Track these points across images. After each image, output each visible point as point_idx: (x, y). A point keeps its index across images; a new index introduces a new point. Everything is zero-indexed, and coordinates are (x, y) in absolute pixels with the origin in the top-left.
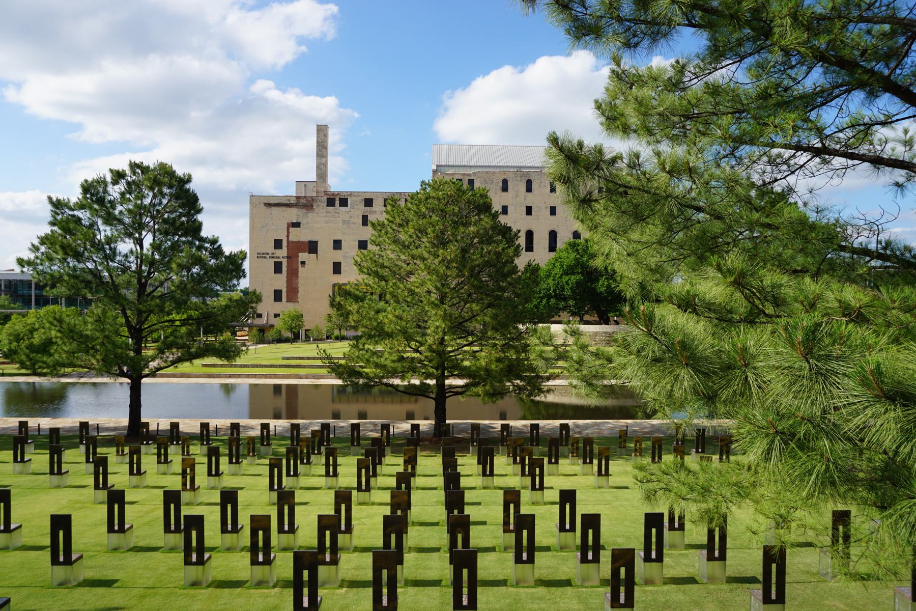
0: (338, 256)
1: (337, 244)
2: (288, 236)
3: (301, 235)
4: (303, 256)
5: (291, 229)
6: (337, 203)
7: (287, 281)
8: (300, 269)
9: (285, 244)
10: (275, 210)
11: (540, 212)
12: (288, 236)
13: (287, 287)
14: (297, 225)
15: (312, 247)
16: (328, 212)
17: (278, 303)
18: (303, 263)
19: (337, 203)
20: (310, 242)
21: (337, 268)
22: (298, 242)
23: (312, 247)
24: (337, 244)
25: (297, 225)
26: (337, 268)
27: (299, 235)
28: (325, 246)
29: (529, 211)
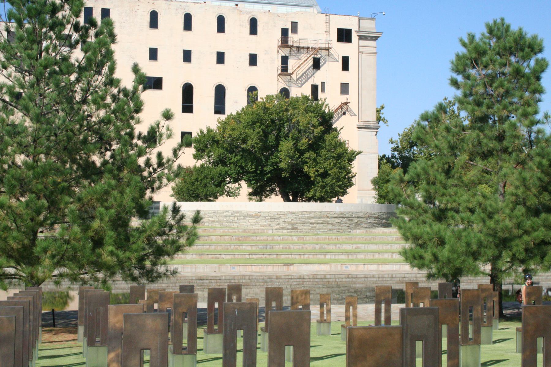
11: (204, 57)
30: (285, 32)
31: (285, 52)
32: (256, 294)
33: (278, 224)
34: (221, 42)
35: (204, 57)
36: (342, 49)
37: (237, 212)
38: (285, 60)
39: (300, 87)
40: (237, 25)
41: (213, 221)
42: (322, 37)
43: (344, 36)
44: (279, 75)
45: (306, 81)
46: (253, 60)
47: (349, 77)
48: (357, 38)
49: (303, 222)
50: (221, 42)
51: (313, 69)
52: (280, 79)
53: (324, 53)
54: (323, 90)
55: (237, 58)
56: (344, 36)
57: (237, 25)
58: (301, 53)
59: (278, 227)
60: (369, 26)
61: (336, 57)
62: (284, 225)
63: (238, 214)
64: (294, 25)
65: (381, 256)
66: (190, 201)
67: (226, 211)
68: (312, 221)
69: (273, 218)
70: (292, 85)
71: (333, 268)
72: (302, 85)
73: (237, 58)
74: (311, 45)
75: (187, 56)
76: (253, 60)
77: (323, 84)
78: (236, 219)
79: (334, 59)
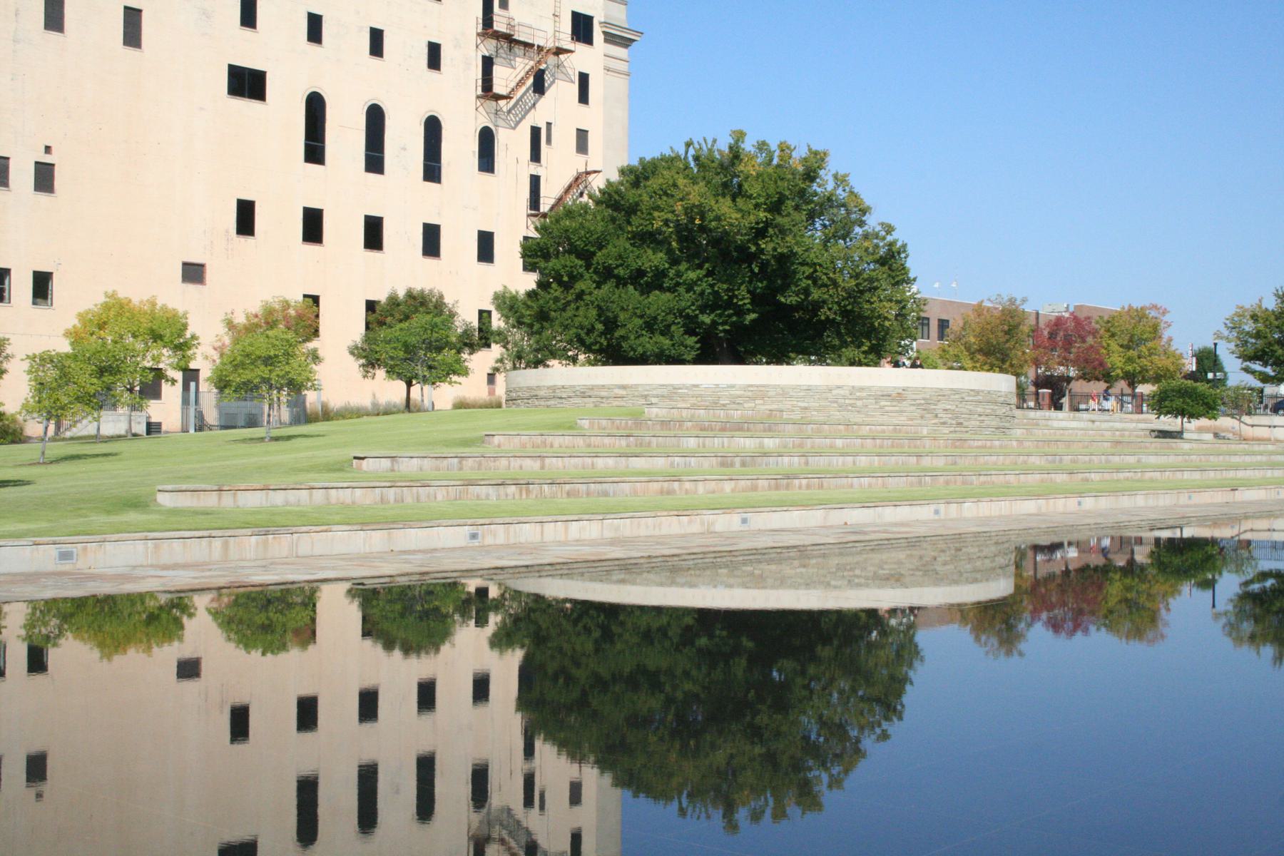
31: (489, 47)
32: (900, 563)
36: (585, 58)
37: (862, 389)
38: (488, 63)
39: (514, 128)
41: (806, 408)
44: (478, 97)
45: (523, 117)
46: (434, 56)
47: (590, 117)
48: (602, 37)
51: (535, 92)
52: (481, 109)
53: (552, 59)
54: (549, 141)
56: (582, 28)
58: (516, 56)
59: (936, 421)
60: (619, 15)
61: (570, 72)
62: (945, 417)
63: (864, 394)
65: (1179, 475)
66: (867, 365)
67: (839, 387)
68: (980, 410)
69: (928, 403)
71: (1183, 499)
72: (518, 123)
76: (434, 56)
77: (549, 124)
78: (859, 403)
79: (567, 75)
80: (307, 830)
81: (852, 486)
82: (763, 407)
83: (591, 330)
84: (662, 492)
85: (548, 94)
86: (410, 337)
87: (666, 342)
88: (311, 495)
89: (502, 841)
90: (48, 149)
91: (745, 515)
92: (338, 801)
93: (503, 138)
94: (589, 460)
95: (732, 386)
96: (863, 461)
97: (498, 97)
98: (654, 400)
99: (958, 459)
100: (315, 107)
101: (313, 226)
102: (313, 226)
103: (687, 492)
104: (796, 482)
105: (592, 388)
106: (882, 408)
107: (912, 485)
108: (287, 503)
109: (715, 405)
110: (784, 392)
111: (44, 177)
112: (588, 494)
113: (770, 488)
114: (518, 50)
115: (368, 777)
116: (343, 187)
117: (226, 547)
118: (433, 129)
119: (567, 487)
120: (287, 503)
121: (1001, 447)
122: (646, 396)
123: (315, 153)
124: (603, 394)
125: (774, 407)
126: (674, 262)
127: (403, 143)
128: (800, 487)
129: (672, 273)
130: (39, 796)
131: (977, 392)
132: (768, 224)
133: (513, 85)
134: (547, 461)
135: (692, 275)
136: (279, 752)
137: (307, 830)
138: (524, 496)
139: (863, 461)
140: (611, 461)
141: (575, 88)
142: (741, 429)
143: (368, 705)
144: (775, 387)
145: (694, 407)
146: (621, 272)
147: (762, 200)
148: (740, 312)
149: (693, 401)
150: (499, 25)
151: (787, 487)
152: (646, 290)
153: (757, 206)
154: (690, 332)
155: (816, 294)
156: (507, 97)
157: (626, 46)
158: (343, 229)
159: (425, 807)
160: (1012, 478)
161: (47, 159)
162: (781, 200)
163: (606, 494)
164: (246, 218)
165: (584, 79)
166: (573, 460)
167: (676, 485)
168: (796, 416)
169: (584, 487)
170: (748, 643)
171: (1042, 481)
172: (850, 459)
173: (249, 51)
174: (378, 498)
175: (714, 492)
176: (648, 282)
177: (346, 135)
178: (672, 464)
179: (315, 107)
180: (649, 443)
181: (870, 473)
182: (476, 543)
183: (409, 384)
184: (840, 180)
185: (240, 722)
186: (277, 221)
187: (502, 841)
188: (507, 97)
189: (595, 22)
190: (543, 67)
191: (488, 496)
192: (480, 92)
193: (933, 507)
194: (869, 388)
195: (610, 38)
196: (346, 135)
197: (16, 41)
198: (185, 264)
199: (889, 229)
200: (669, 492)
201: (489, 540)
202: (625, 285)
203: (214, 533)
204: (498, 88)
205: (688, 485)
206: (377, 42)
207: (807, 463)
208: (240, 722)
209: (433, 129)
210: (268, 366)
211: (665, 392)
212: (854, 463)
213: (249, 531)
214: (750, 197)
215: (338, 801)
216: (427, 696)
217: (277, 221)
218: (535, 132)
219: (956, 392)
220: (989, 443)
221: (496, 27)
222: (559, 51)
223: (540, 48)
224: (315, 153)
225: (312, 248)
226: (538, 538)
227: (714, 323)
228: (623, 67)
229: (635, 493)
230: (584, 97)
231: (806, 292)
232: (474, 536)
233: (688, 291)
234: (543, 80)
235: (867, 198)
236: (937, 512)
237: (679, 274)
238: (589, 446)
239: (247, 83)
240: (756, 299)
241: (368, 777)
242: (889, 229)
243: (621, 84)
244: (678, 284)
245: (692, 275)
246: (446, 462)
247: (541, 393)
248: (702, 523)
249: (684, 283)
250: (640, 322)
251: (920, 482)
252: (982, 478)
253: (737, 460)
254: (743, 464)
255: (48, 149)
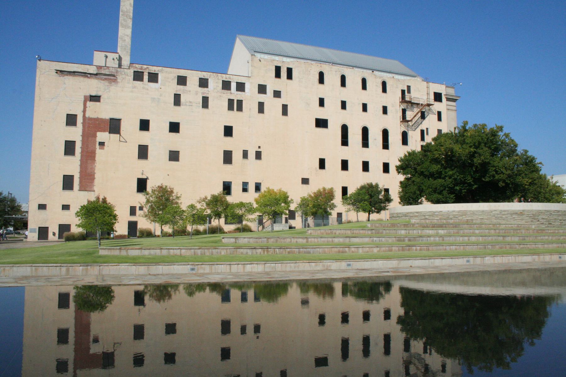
0: (144, 138)
1: (145, 125)
2: (84, 111)
3: (102, 111)
4: (102, 136)
5: (89, 104)
6: (146, 77)
7: (81, 166)
8: (98, 151)
9: (80, 120)
10: (69, 80)
11: (354, 107)
12: (84, 111)
13: (81, 172)
14: (96, 98)
15: (114, 126)
16: (135, 87)
17: (68, 193)
18: (102, 144)
19: (146, 77)
20: (111, 119)
21: (143, 152)
22: (97, 119)
23: (114, 126)
24: (145, 125)
25: (96, 98)
26: (143, 152)
27: (98, 111)
28: (130, 126)
29: (344, 105)
30: (403, 92)
31: (404, 106)
33: (538, 221)
34: (365, 97)
35: (354, 107)
37: (505, 211)
38: (404, 111)
40: (374, 84)
42: (425, 97)
43: (438, 97)
44: (401, 122)
46: (385, 110)
49: (555, 219)
50: (365, 97)
53: (427, 108)
54: (427, 134)
55: (375, 109)
56: (438, 97)
57: (374, 84)
60: (451, 92)
62: (542, 221)
64: (409, 87)
67: (495, 211)
68: (560, 218)
69: (534, 216)
70: (409, 129)
72: (416, 129)
73: (375, 109)
74: (421, 103)
75: (344, 105)
76: (385, 110)
77: (427, 129)
78: (504, 216)
79: (433, 112)
80: (345, 354)
81: (446, 249)
82: (465, 218)
83: (415, 193)
84: (339, 252)
85: (426, 119)
86: (371, 199)
87: (441, 196)
88: (161, 252)
89: (415, 364)
90: (259, 147)
91: (349, 263)
92: (356, 346)
93: (410, 134)
94: (331, 239)
95: (454, 211)
96: (473, 239)
97: (408, 121)
98: (427, 217)
99: (526, 238)
100: (345, 129)
101: (345, 165)
102: (345, 165)
103: (353, 252)
104: (414, 248)
105: (408, 213)
106: (514, 218)
107: (480, 249)
108: (150, 254)
109: (448, 218)
110: (473, 213)
111: (258, 155)
112: (299, 252)
113: (399, 250)
114: (414, 106)
115: (366, 340)
116: (355, 153)
117: (68, 270)
118: (385, 133)
119: (288, 250)
120: (150, 254)
121: (563, 232)
122: (424, 216)
123: (345, 142)
124: (411, 215)
125: (470, 218)
126: (445, 168)
127: (375, 138)
128: (416, 250)
129: (443, 173)
130: (258, 337)
131: (559, 211)
132: (475, 152)
133: (412, 117)
134: (310, 240)
135: (451, 173)
136: (335, 330)
137: (345, 354)
138: (266, 253)
139: (473, 239)
140: (341, 240)
141: (436, 116)
142: (441, 227)
143: (345, 318)
144: (470, 211)
145: (440, 219)
146: (426, 173)
147: (472, 144)
148: (470, 185)
149: (440, 217)
150: (407, 99)
151: (409, 250)
152: (435, 179)
153: (470, 147)
154: (451, 193)
155: (497, 177)
156: (411, 121)
157: (455, 102)
158: (355, 165)
159: (387, 351)
160: (540, 246)
161: (259, 150)
162: (480, 143)
163: (309, 253)
164: (322, 164)
165: (439, 114)
166: (322, 239)
167: (347, 249)
168: (478, 222)
169: (297, 250)
170: (477, 305)
171: (558, 247)
172: (466, 238)
173: (322, 114)
174: (193, 253)
175: (368, 252)
176: (437, 175)
177: (355, 137)
178: (373, 241)
179: (345, 129)
180: (382, 233)
181: (460, 244)
182: (194, 272)
183: (369, 214)
184: (507, 135)
185: (322, 319)
186: (333, 165)
187: (415, 364)
188: (411, 121)
189: (443, 95)
190: (424, 110)
191: (247, 253)
192: (401, 120)
193: (465, 259)
194: (508, 211)
195: (448, 99)
196: (355, 137)
197: (250, 117)
198: (302, 179)
199: (526, 151)
200: (343, 252)
201: (201, 271)
202: (429, 178)
203: (63, 265)
204: (408, 118)
205: (353, 249)
206: (365, 108)
207: (443, 240)
208: (322, 319)
209: (385, 133)
210: (318, 208)
211: (430, 214)
212: (469, 240)
213: (79, 265)
214: (468, 143)
215: (356, 346)
216: (366, 316)
217: (333, 165)
218: (422, 132)
219: (547, 211)
220: (556, 231)
221: (407, 99)
222: (429, 105)
223: (422, 105)
224: (345, 142)
225: (345, 172)
226: (242, 271)
227: (461, 190)
228: (454, 108)
229: (325, 252)
230: (440, 119)
231: (494, 176)
232: (193, 269)
233: (450, 178)
234: (424, 115)
235: (517, 141)
236: (468, 261)
237: (446, 173)
238: (353, 233)
239: (321, 123)
240: (476, 180)
241: (366, 340)
242: (526, 151)
243: (454, 114)
244: (446, 176)
245: (451, 173)
246: (260, 240)
247: (395, 215)
248: (324, 266)
249: (448, 176)
250: (431, 190)
251: (485, 248)
252: (521, 246)
253: (407, 239)
254: (409, 240)
255: (259, 147)
